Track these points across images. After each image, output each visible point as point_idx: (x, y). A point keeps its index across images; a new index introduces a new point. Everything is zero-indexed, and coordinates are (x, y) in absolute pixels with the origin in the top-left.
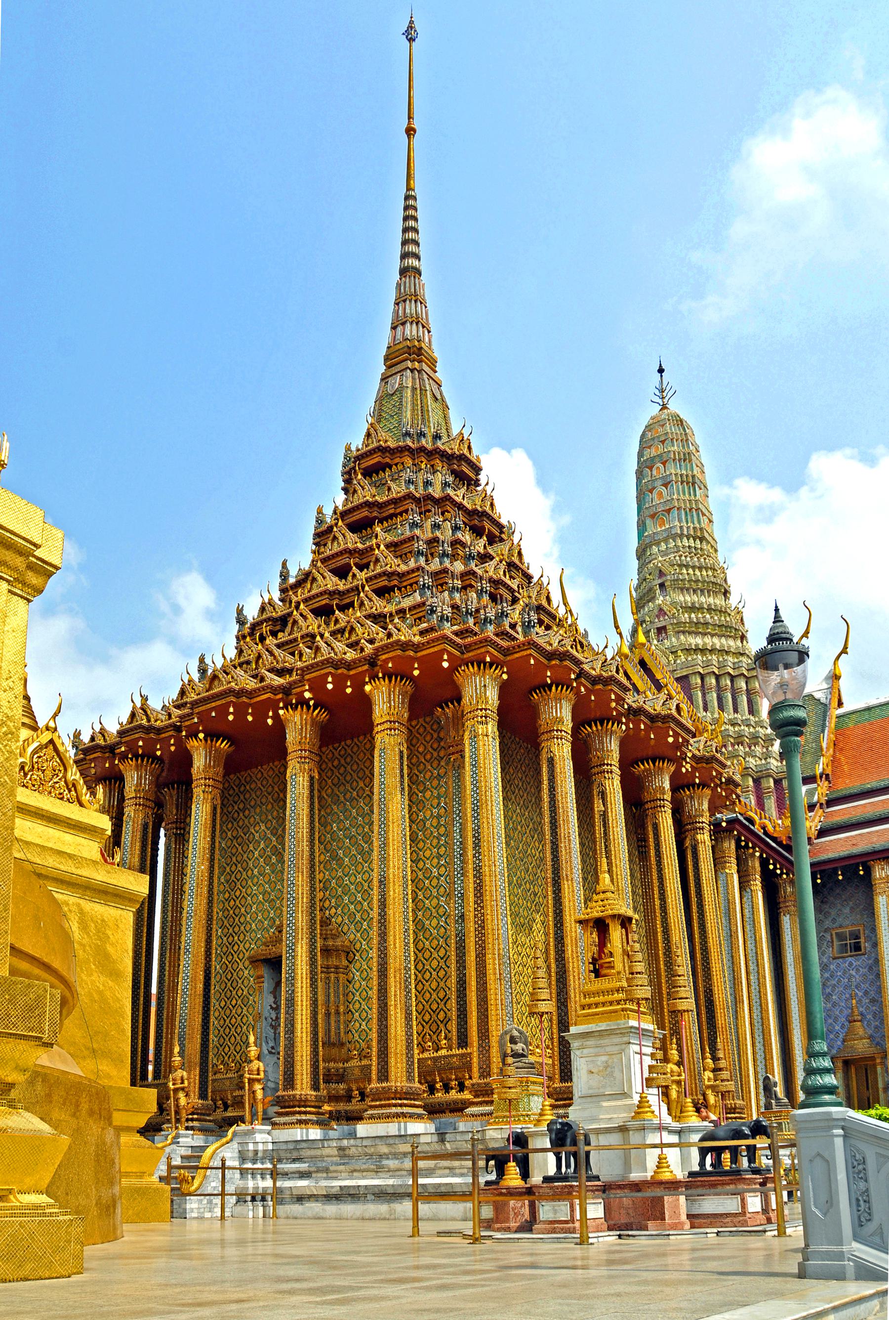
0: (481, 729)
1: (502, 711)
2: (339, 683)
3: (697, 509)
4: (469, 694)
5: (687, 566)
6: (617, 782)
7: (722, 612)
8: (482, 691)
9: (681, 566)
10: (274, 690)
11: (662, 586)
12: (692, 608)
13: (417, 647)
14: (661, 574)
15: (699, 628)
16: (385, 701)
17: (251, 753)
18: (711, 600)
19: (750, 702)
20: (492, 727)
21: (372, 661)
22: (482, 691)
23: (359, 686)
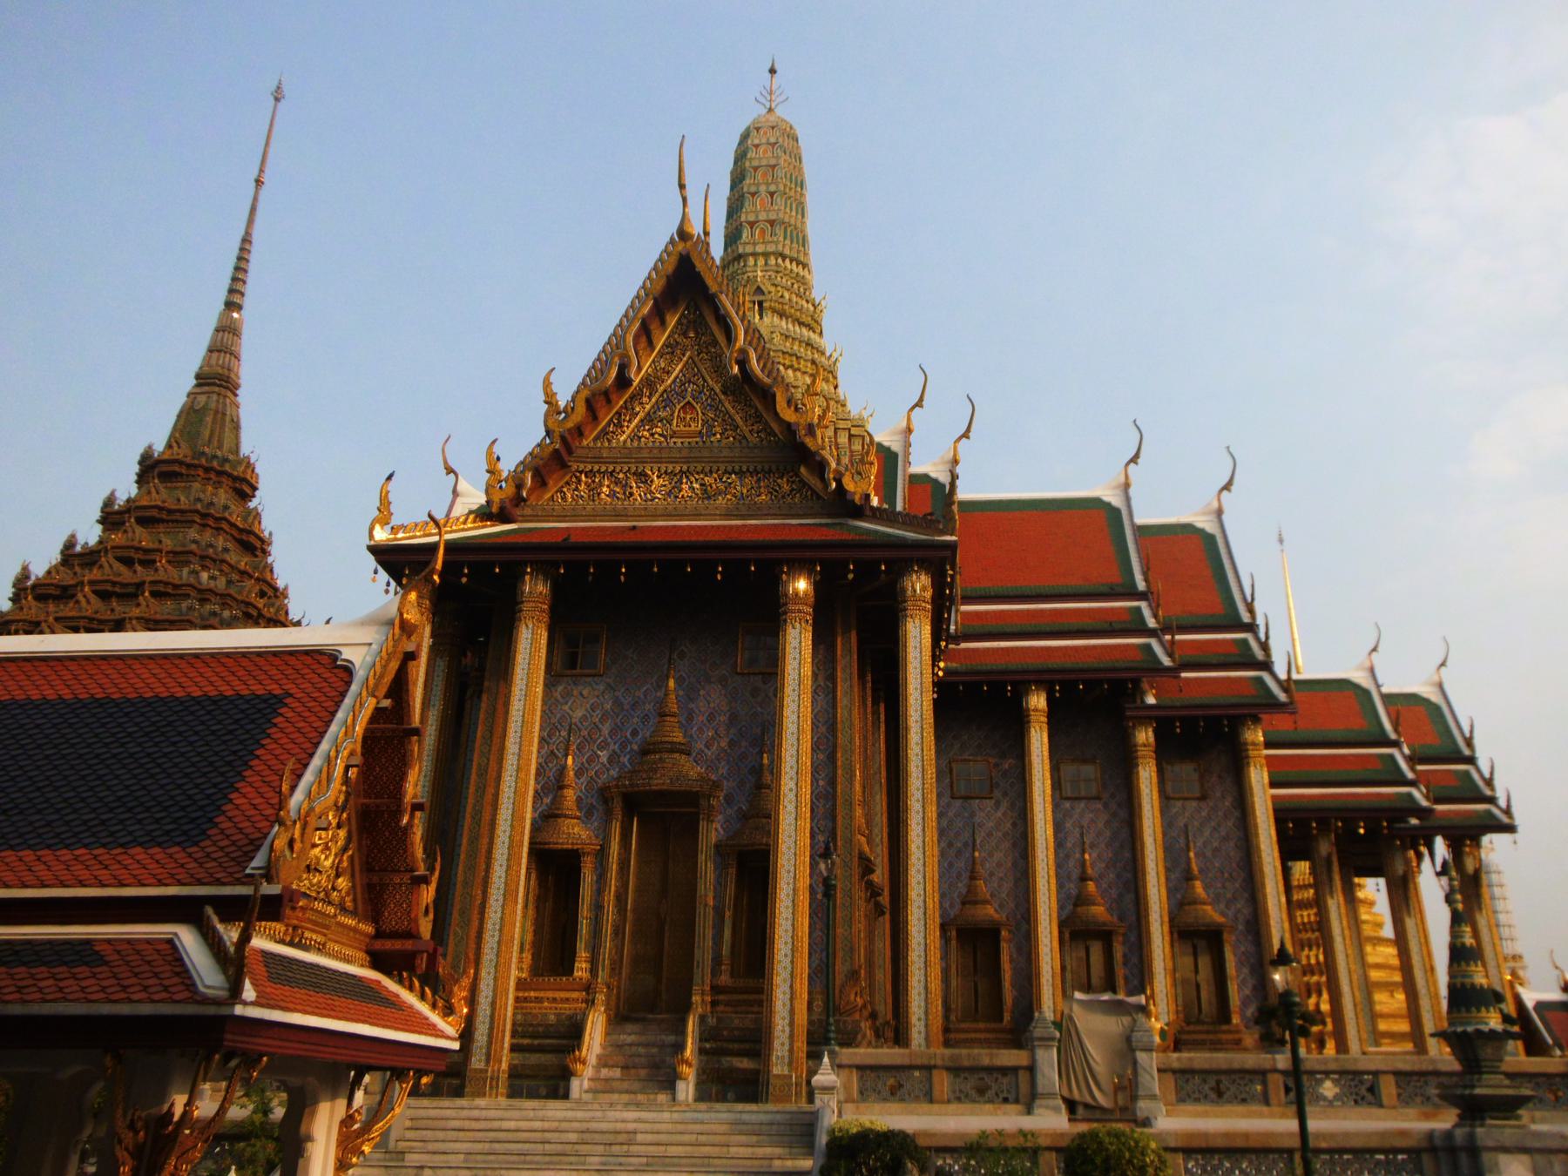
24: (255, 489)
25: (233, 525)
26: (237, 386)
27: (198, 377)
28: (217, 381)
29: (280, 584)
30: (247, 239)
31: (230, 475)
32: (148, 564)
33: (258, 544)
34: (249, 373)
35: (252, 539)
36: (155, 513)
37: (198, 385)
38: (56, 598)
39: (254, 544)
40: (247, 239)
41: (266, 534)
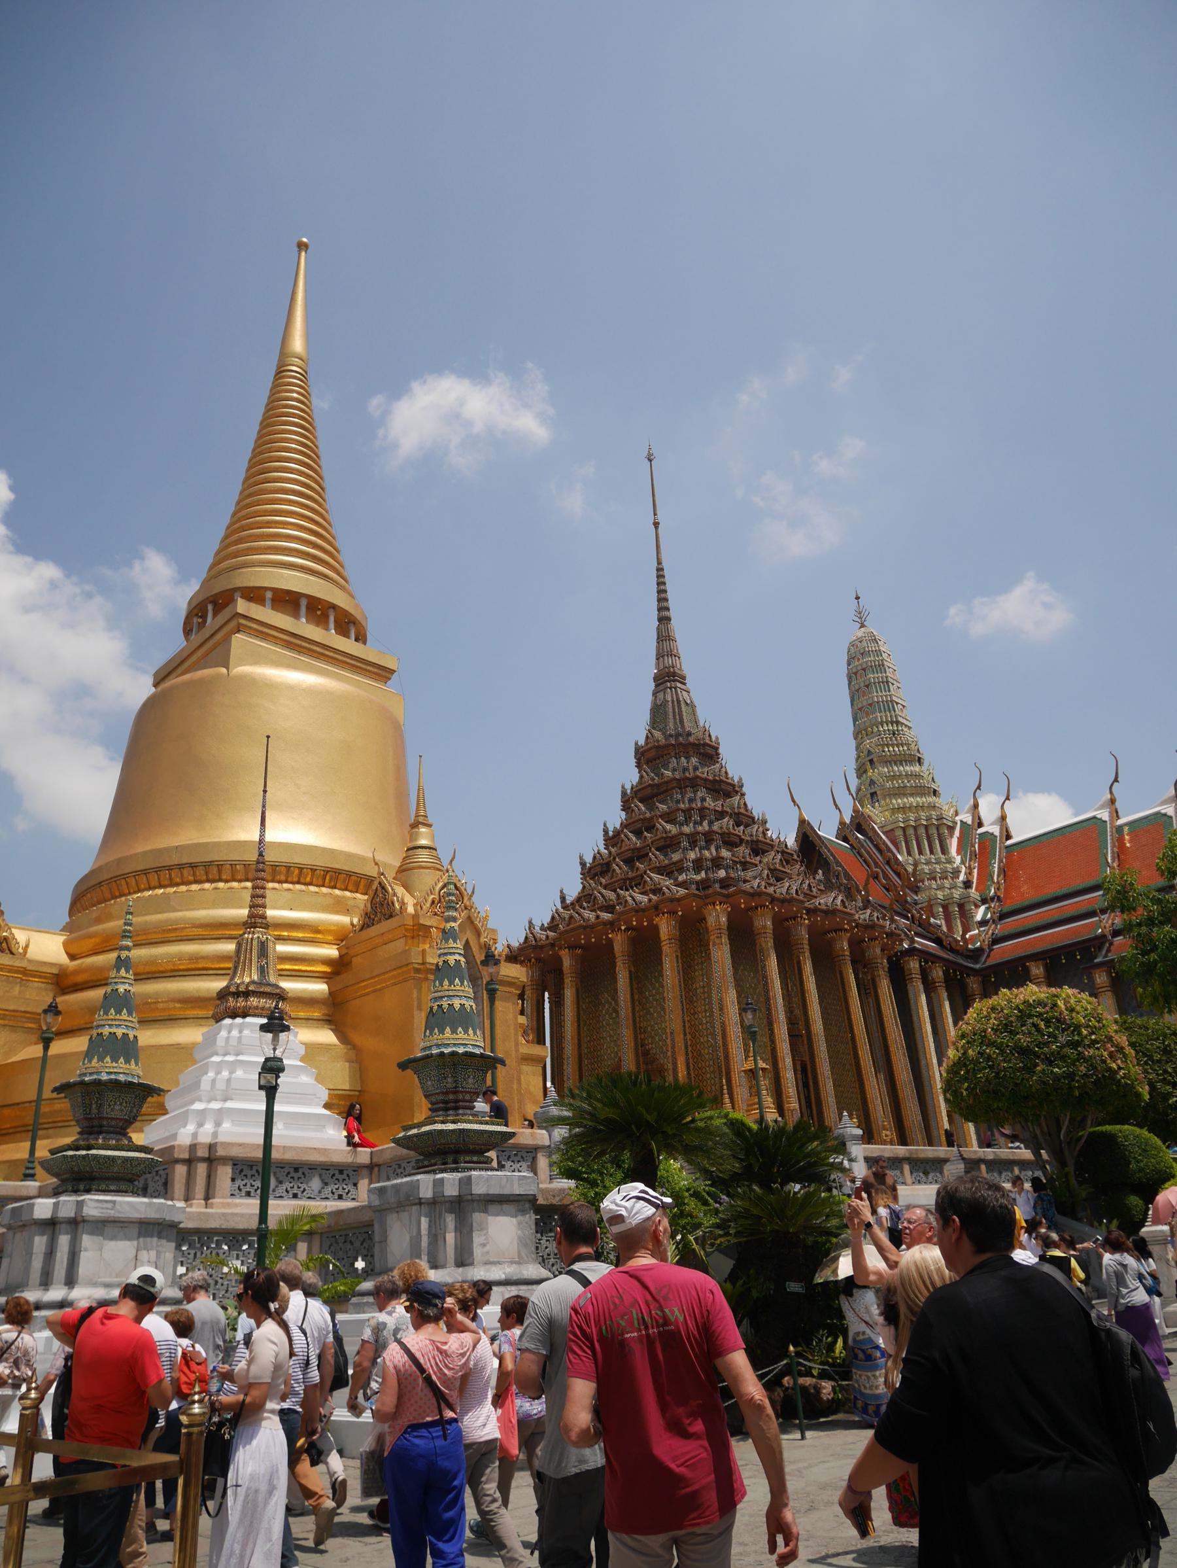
0: (717, 941)
1: (729, 928)
2: (640, 922)
3: (892, 701)
4: (711, 921)
5: (888, 745)
6: (807, 954)
7: (918, 776)
8: (717, 916)
9: (883, 746)
10: (605, 923)
11: (871, 761)
12: (894, 777)
13: (679, 900)
14: (869, 752)
15: (900, 792)
16: (666, 927)
17: (595, 964)
18: (908, 768)
19: (941, 842)
20: (725, 939)
21: (656, 907)
22: (717, 916)
23: (650, 921)
24: (717, 749)
25: (706, 780)
26: (684, 678)
27: (655, 679)
28: (668, 678)
29: (756, 813)
30: (660, 570)
31: (694, 744)
32: (651, 828)
33: (730, 789)
34: (688, 664)
35: (723, 786)
36: (649, 791)
37: (656, 686)
38: (603, 873)
39: (725, 789)
40: (660, 570)
41: (736, 780)
